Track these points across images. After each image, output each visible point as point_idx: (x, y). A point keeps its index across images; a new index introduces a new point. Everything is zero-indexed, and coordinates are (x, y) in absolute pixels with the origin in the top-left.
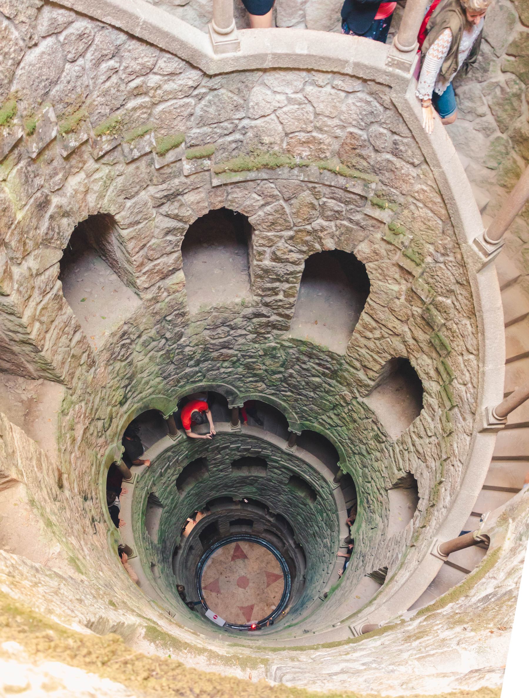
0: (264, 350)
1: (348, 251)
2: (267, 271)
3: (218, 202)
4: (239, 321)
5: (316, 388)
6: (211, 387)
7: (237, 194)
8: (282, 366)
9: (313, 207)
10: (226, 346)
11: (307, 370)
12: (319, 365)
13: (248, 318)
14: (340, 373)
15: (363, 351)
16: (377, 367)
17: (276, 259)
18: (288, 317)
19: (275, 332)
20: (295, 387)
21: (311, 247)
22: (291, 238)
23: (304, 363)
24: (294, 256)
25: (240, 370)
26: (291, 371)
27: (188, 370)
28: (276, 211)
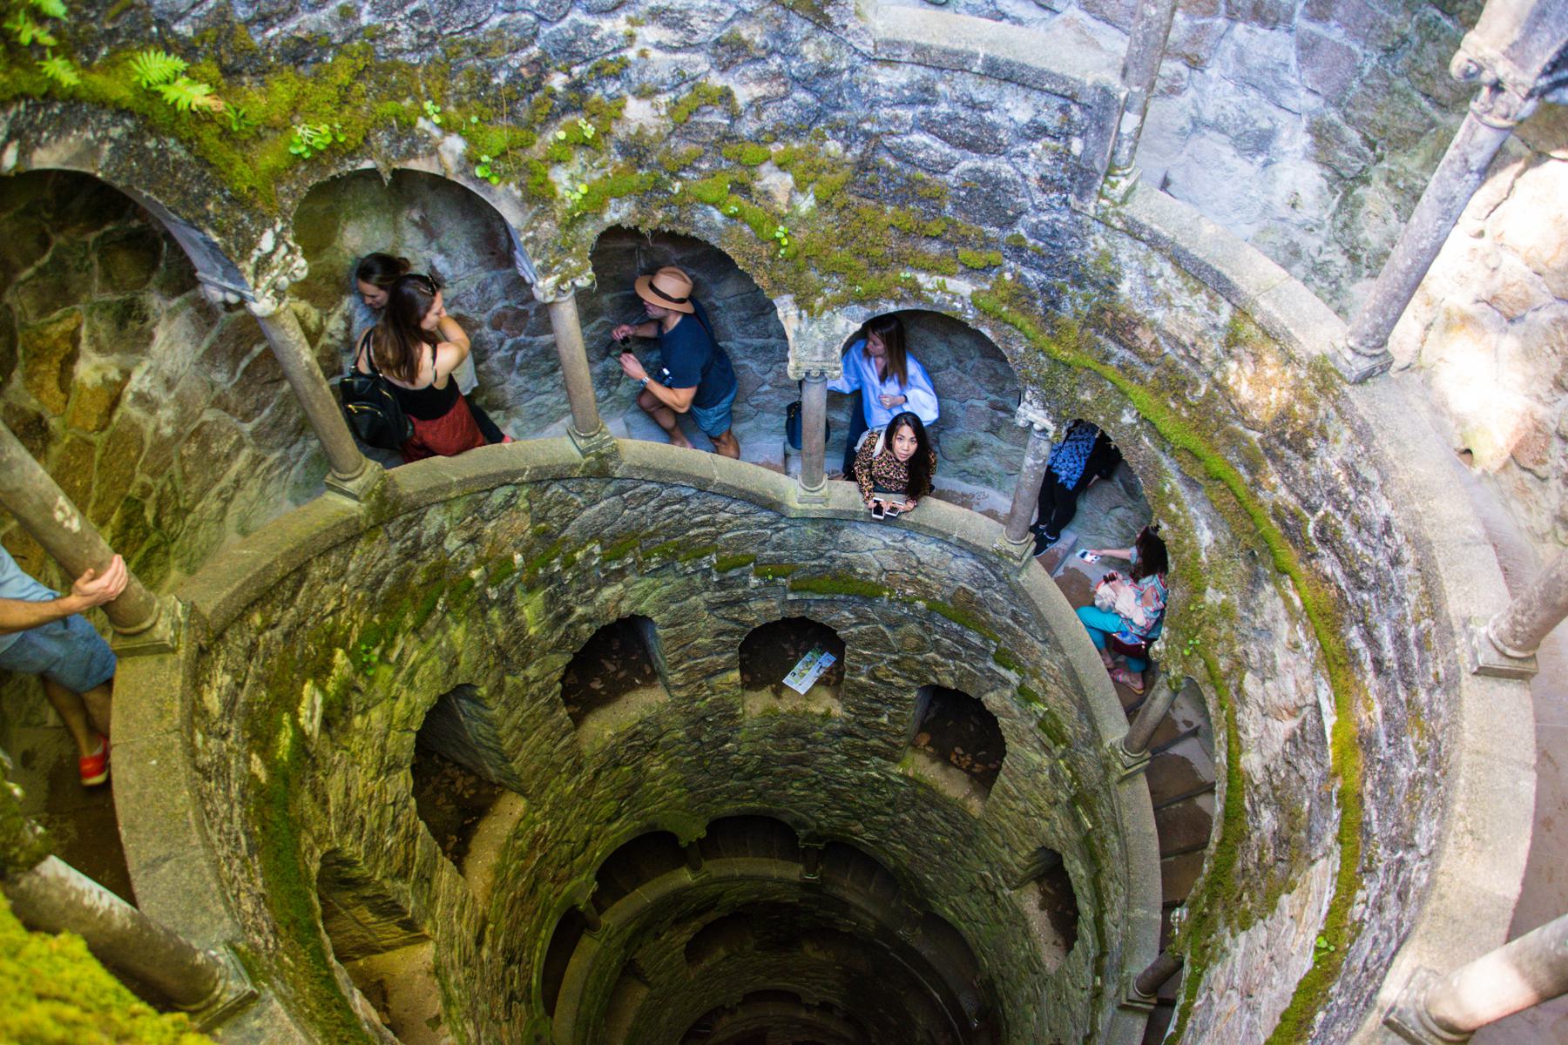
0: (860, 779)
1: (973, 694)
2: (863, 688)
3: (795, 613)
4: (820, 734)
5: (943, 852)
6: (771, 811)
7: (822, 609)
8: (890, 804)
9: (924, 640)
10: (799, 760)
11: (929, 822)
12: (946, 820)
13: (837, 735)
14: (976, 842)
15: (1004, 821)
16: (1025, 853)
17: (875, 678)
18: (895, 746)
19: (877, 759)
20: (909, 839)
21: (922, 678)
22: (896, 662)
23: (925, 811)
24: (901, 682)
25: (821, 795)
26: (903, 816)
27: (732, 783)
28: (874, 633)
